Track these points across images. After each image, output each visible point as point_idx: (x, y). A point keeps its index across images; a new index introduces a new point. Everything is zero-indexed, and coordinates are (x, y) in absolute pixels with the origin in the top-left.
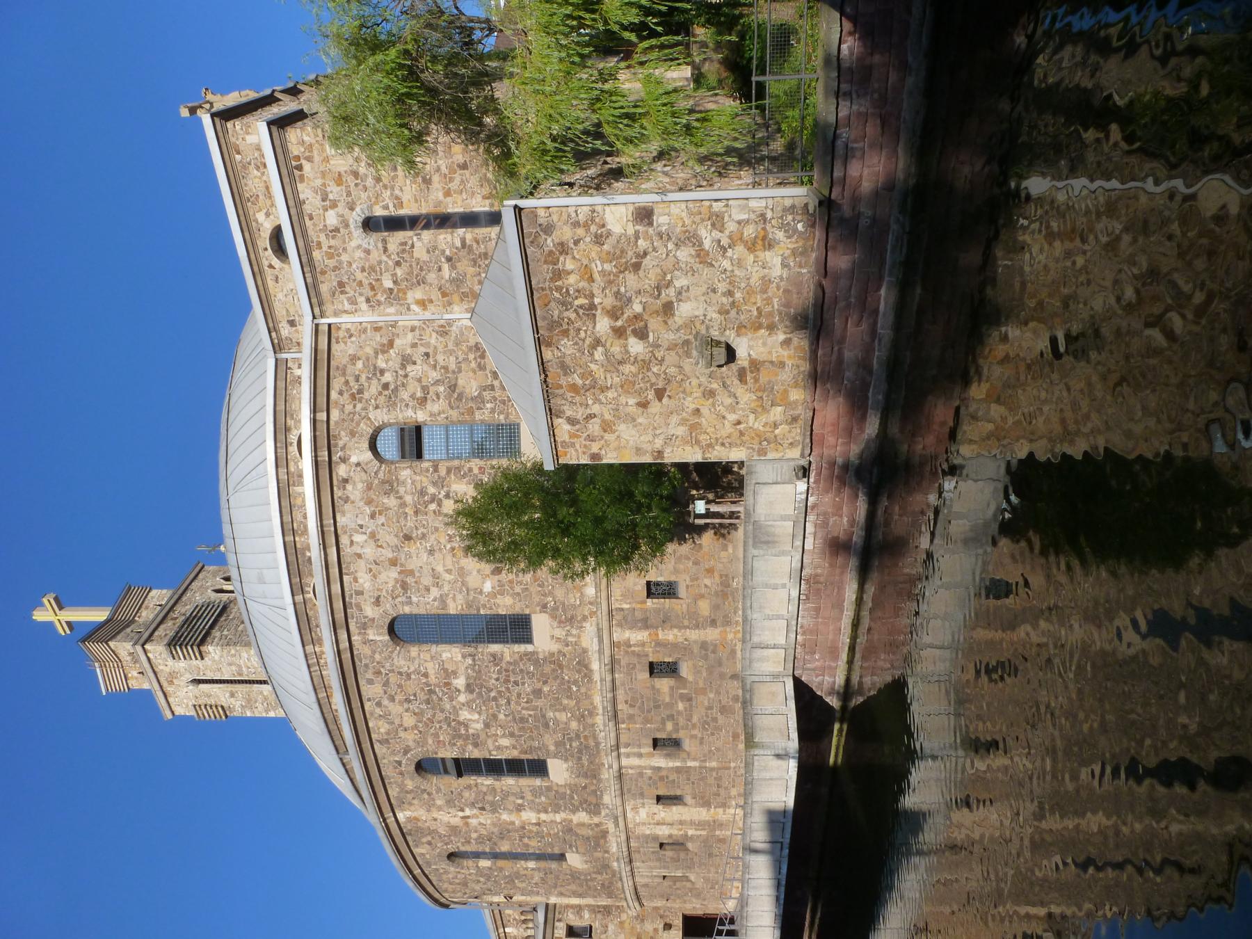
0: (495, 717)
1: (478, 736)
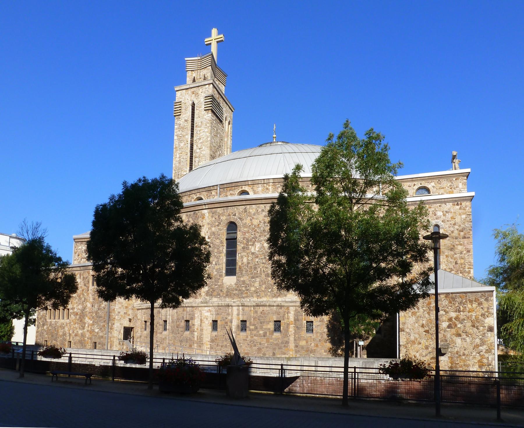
0: (257, 257)
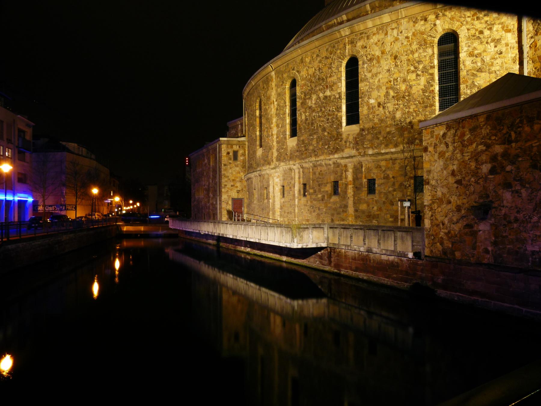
0: (314, 111)
1: (305, 104)
